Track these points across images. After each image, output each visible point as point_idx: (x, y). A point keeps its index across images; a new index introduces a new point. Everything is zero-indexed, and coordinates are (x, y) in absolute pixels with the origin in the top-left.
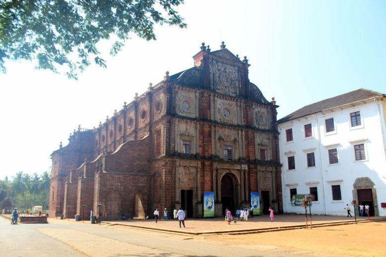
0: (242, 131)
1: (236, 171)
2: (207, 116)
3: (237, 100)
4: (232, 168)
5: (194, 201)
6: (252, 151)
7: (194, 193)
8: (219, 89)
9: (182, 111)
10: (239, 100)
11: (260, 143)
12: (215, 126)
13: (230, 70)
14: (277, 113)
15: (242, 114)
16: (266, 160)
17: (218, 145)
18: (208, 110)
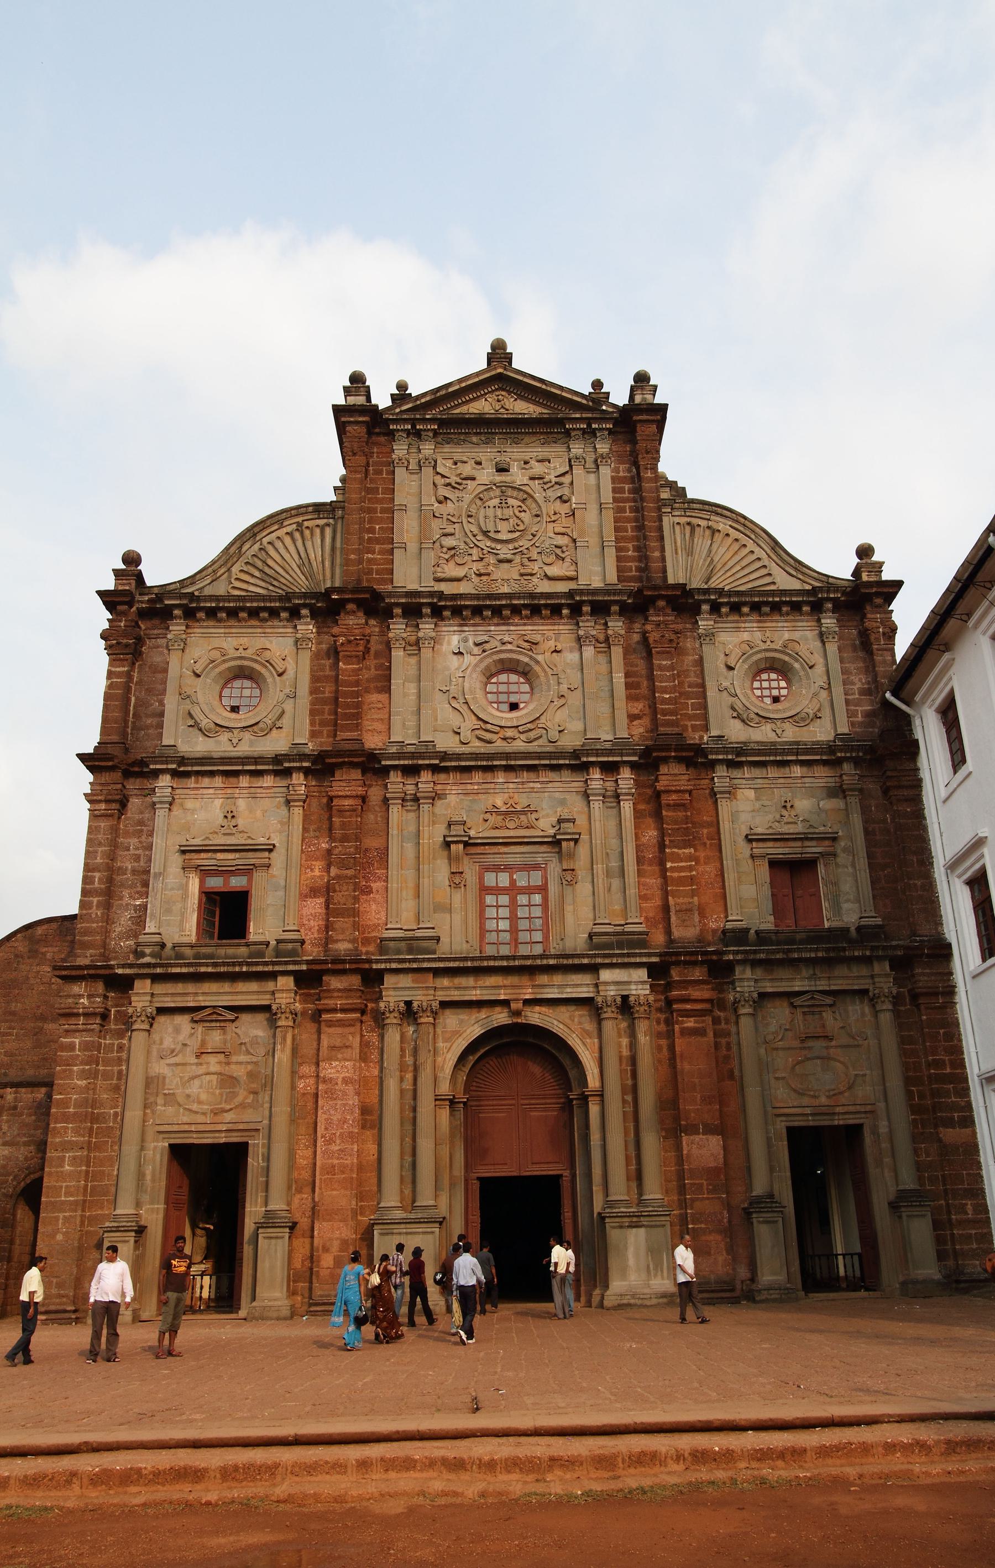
0: (610, 768)
1: (564, 1013)
2: (357, 727)
3: (576, 610)
4: (528, 994)
5: (253, 1211)
6: (692, 878)
7: (254, 1163)
8: (459, 580)
9: (204, 723)
10: (586, 609)
11: (759, 830)
12: (411, 771)
13: (538, 469)
14: (894, 629)
15: (619, 678)
16: (827, 925)
17: (441, 871)
18: (374, 697)
